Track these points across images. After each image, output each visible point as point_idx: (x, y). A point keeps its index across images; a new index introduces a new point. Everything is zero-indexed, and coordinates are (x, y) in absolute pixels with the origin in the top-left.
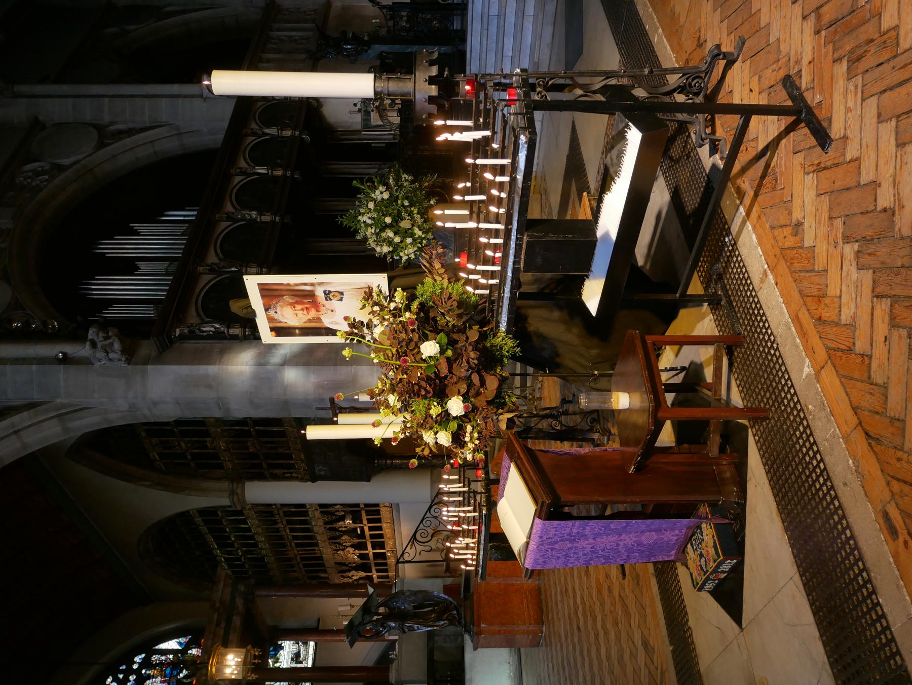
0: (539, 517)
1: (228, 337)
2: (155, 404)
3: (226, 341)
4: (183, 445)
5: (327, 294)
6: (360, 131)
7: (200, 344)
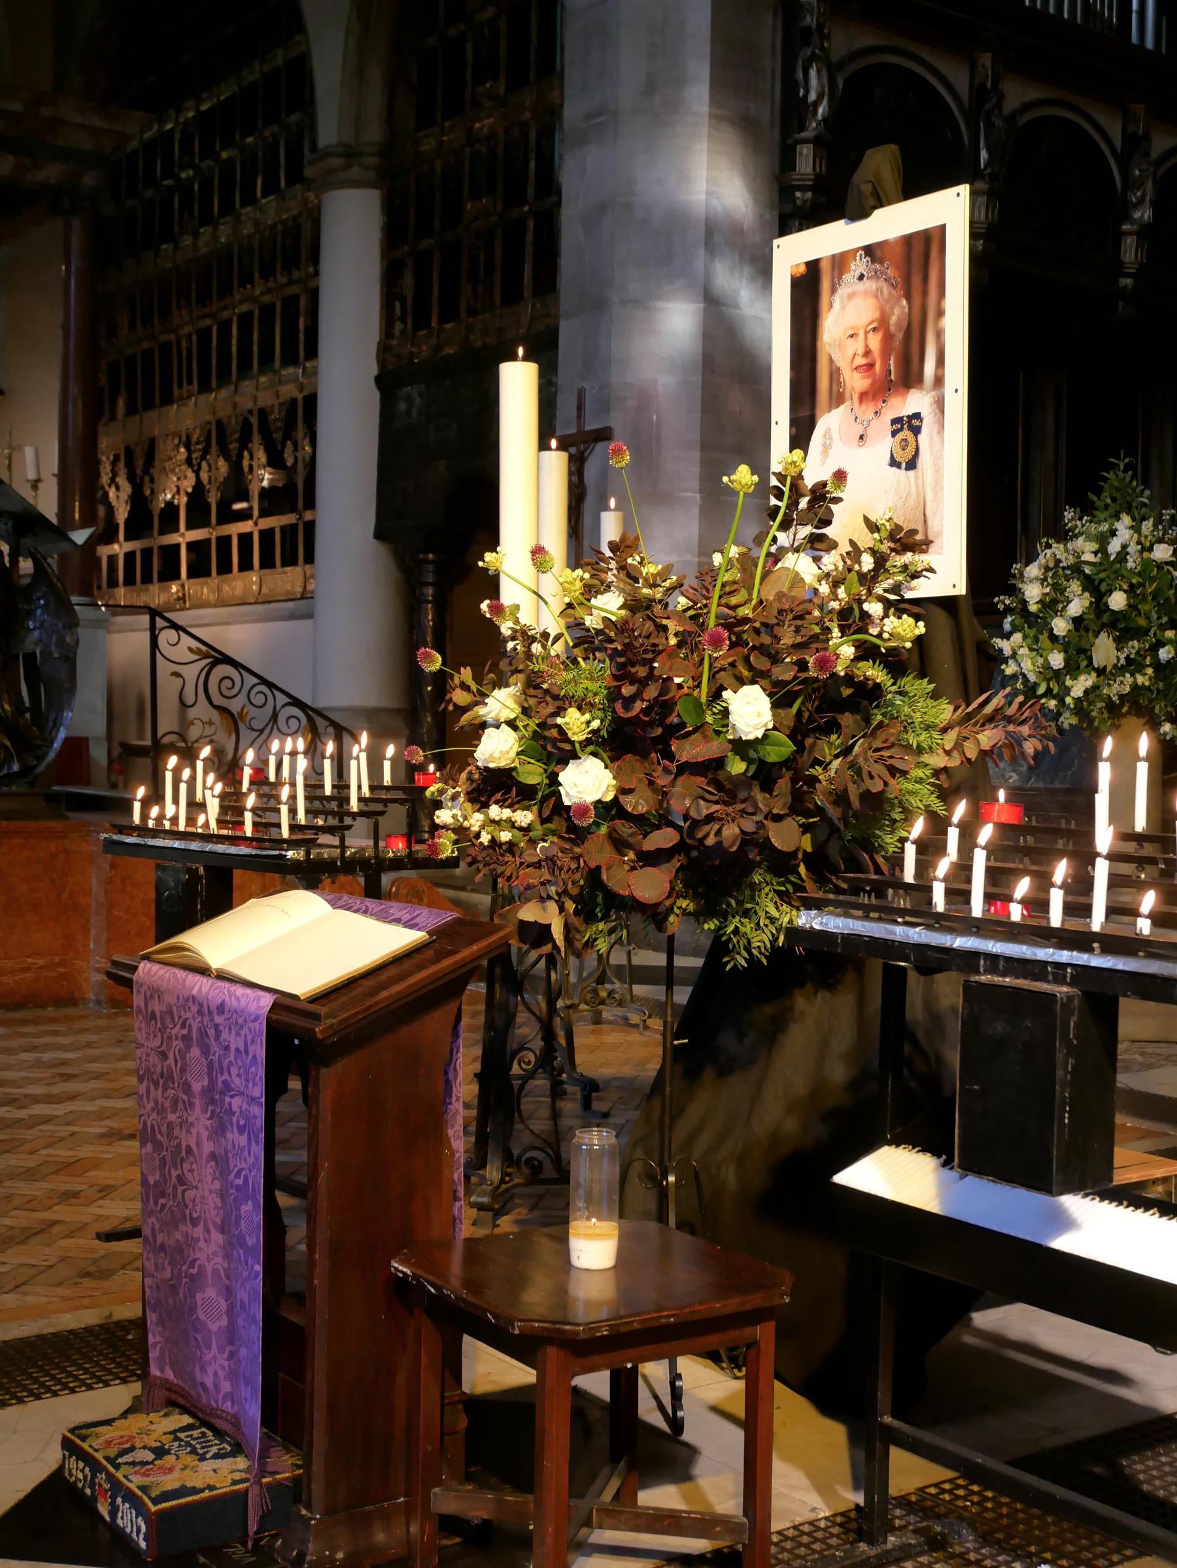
0: (275, 1006)
1: (790, 142)
3: (777, 134)
4: (488, 13)
5: (911, 424)
7: (771, 63)
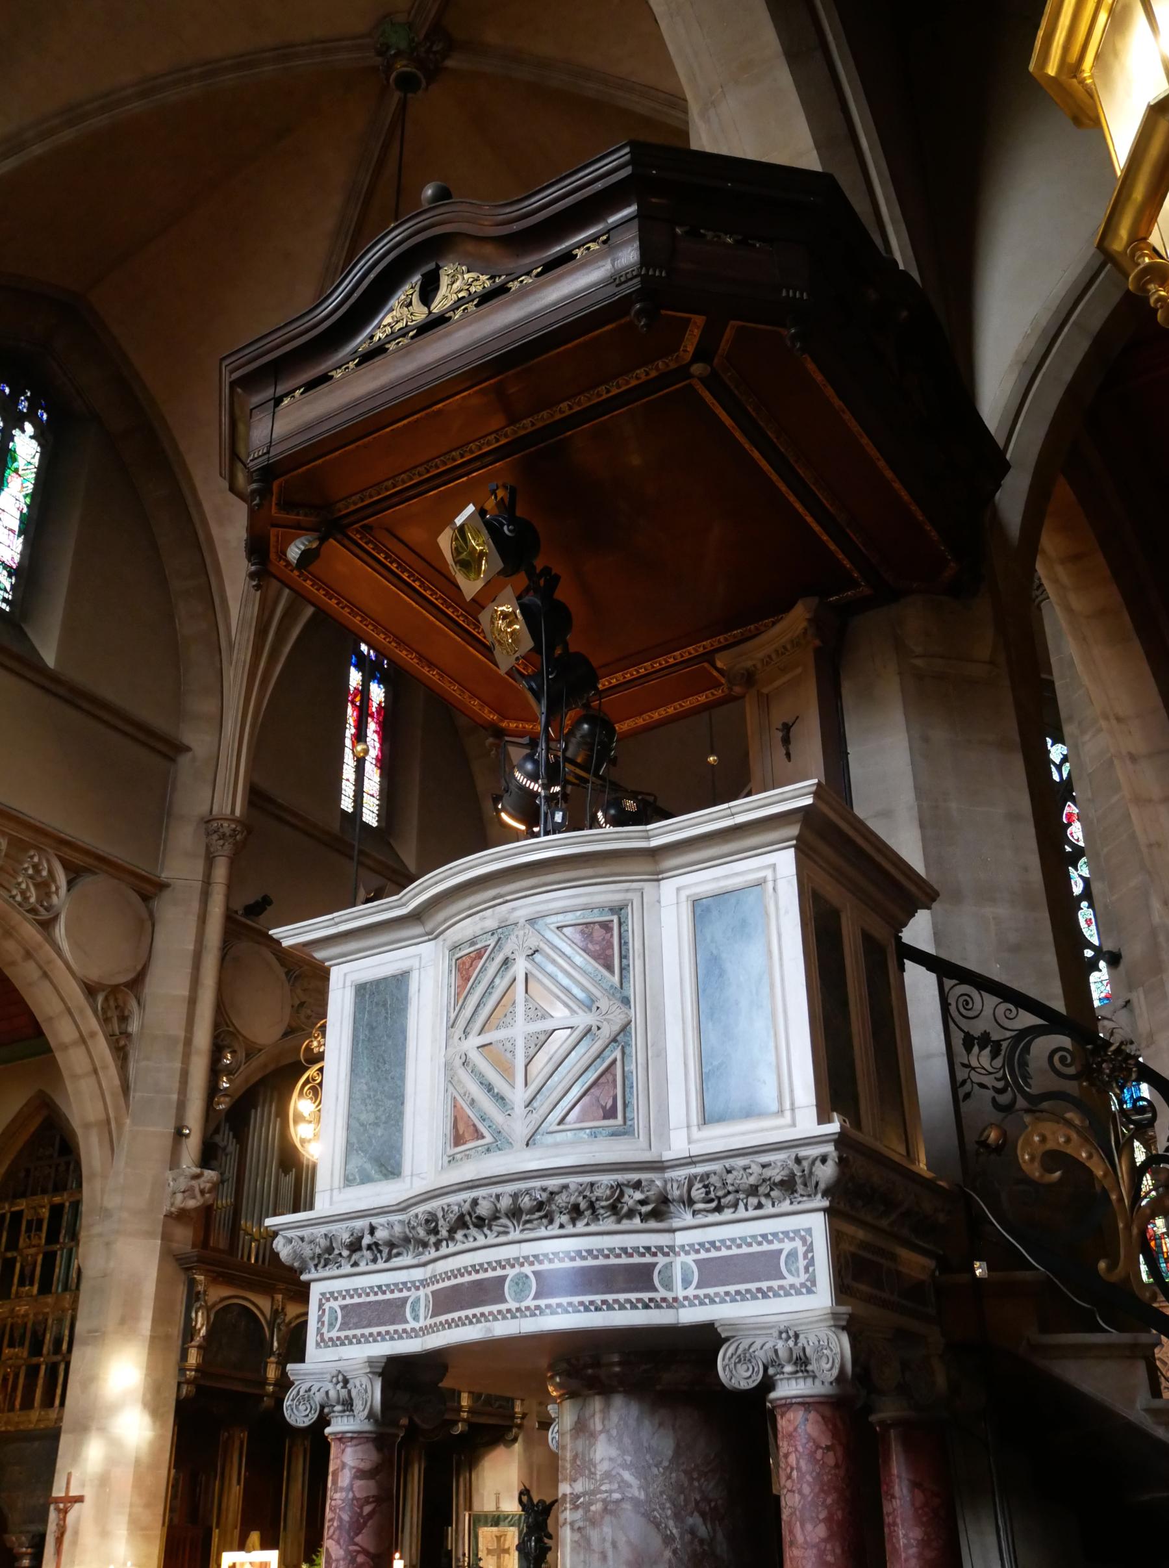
1: (186, 1346)
2: (108, 1244)
3: (180, 1342)
4: (32, 1251)
6: (470, 1509)
7: (181, 1308)
